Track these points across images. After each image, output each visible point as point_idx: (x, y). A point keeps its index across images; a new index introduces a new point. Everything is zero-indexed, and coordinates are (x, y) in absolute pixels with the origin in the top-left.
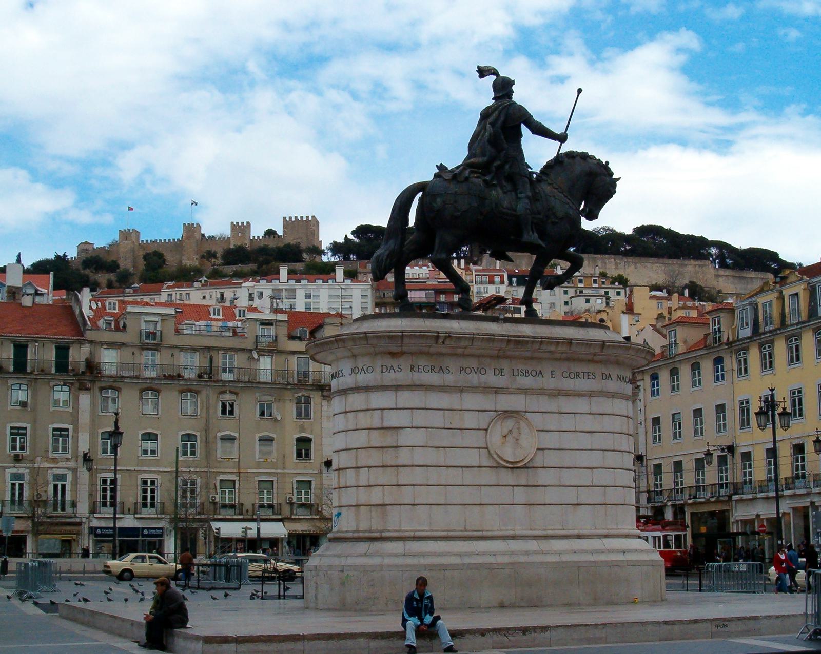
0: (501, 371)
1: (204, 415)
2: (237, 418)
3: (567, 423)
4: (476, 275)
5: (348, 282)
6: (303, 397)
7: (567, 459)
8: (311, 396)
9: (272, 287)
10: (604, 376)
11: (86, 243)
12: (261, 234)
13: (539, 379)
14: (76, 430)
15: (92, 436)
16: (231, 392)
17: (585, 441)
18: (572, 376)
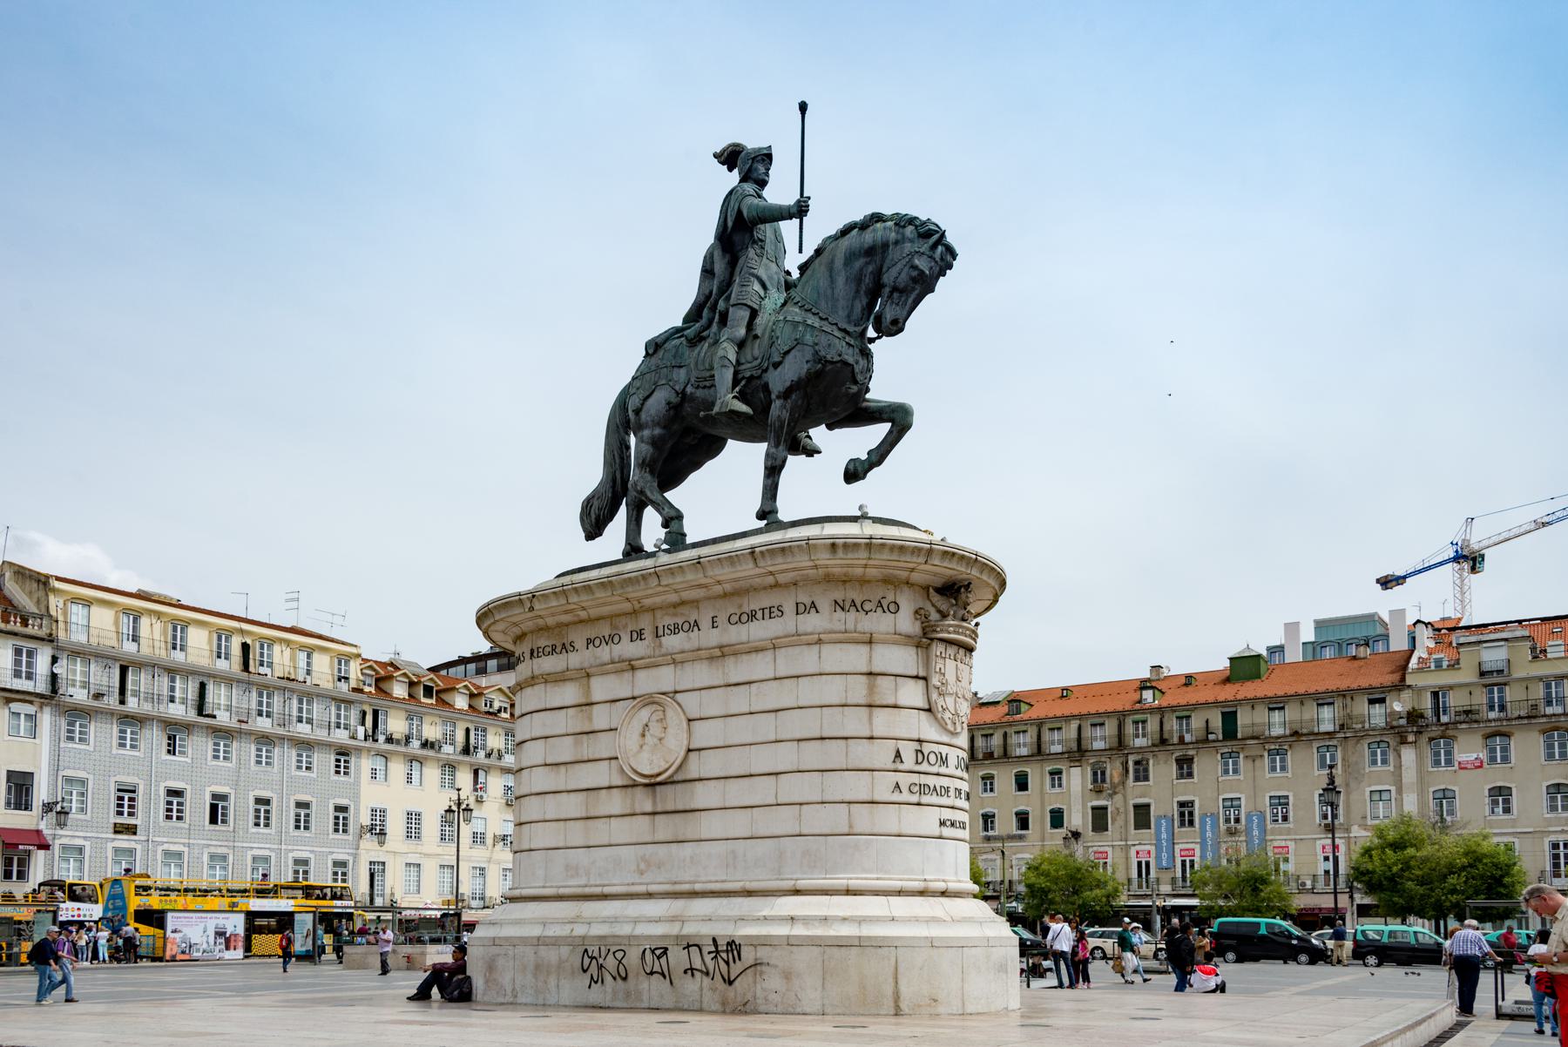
0: (640, 635)
3: (739, 700)
7: (736, 762)
10: (801, 608)
13: (695, 634)
14: (1400, 791)
15: (1421, 793)
17: (766, 727)
18: (745, 618)
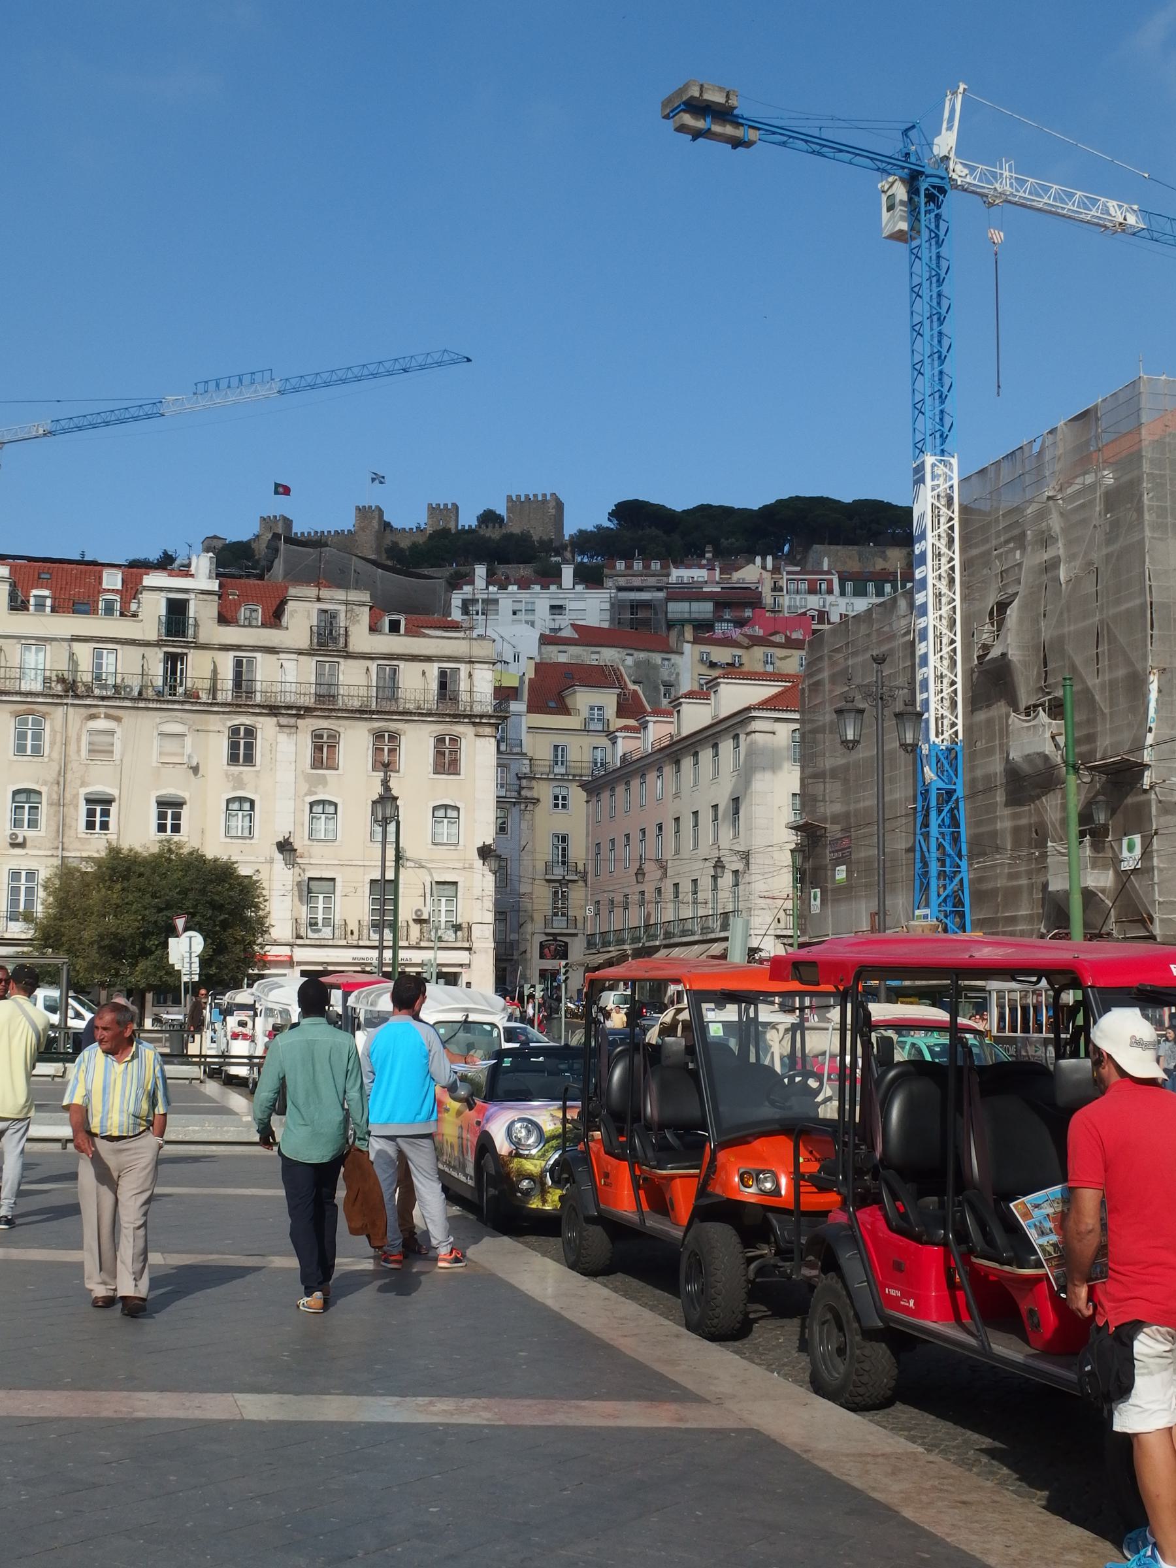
1: (55, 755)
2: (118, 763)
4: (788, 580)
5: (579, 588)
6: (242, 728)
8: (258, 726)
9: (460, 596)
11: (215, 537)
12: (474, 523)
16: (107, 716)
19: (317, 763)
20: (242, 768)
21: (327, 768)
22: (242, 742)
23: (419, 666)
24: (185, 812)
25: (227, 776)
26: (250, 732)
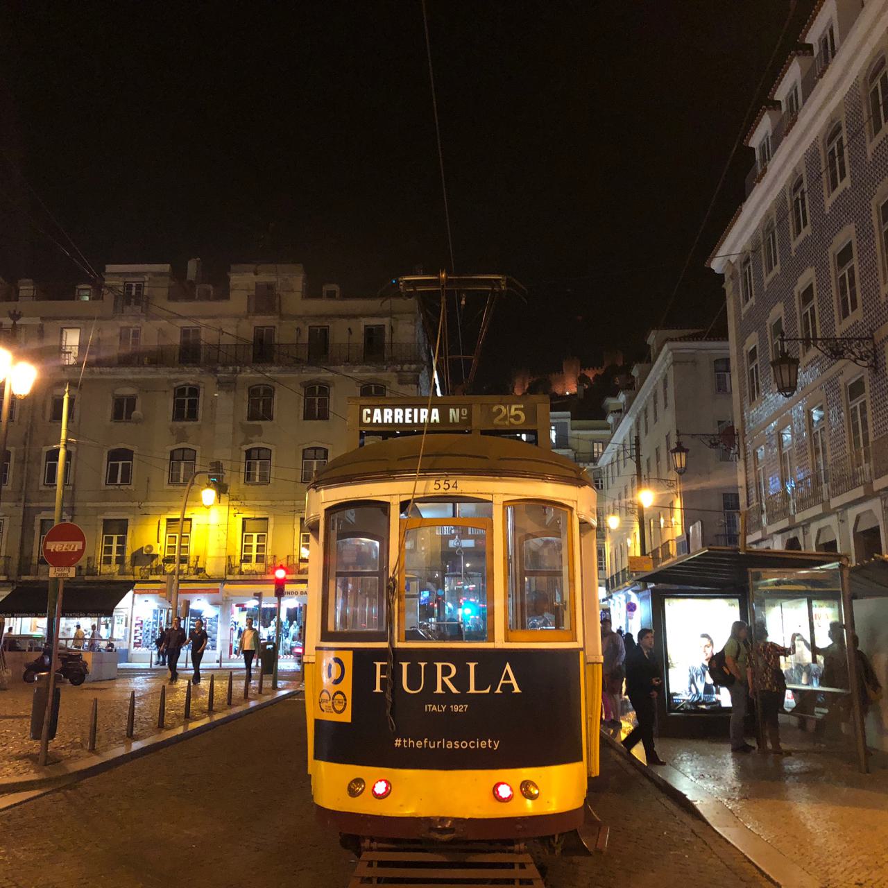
8: (202, 385)
19: (252, 416)
20: (185, 423)
21: (264, 419)
22: (187, 399)
23: (346, 323)
24: (135, 464)
25: (171, 429)
26: (194, 391)
